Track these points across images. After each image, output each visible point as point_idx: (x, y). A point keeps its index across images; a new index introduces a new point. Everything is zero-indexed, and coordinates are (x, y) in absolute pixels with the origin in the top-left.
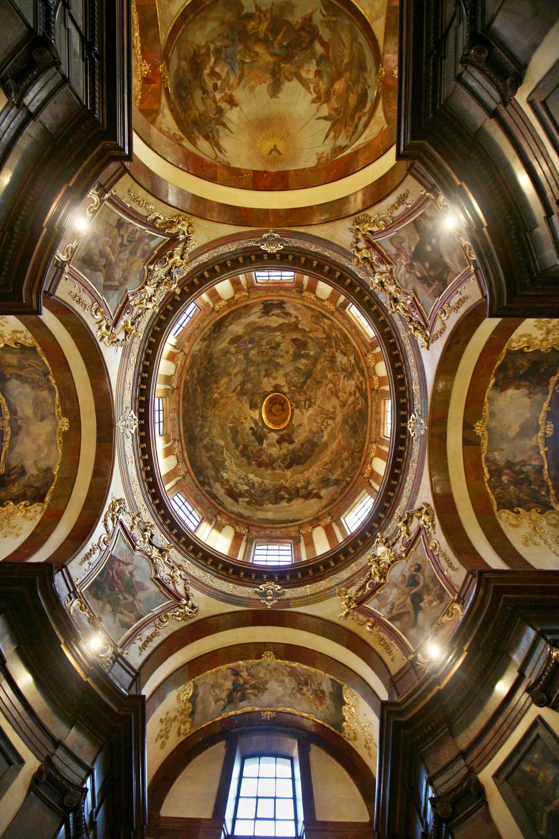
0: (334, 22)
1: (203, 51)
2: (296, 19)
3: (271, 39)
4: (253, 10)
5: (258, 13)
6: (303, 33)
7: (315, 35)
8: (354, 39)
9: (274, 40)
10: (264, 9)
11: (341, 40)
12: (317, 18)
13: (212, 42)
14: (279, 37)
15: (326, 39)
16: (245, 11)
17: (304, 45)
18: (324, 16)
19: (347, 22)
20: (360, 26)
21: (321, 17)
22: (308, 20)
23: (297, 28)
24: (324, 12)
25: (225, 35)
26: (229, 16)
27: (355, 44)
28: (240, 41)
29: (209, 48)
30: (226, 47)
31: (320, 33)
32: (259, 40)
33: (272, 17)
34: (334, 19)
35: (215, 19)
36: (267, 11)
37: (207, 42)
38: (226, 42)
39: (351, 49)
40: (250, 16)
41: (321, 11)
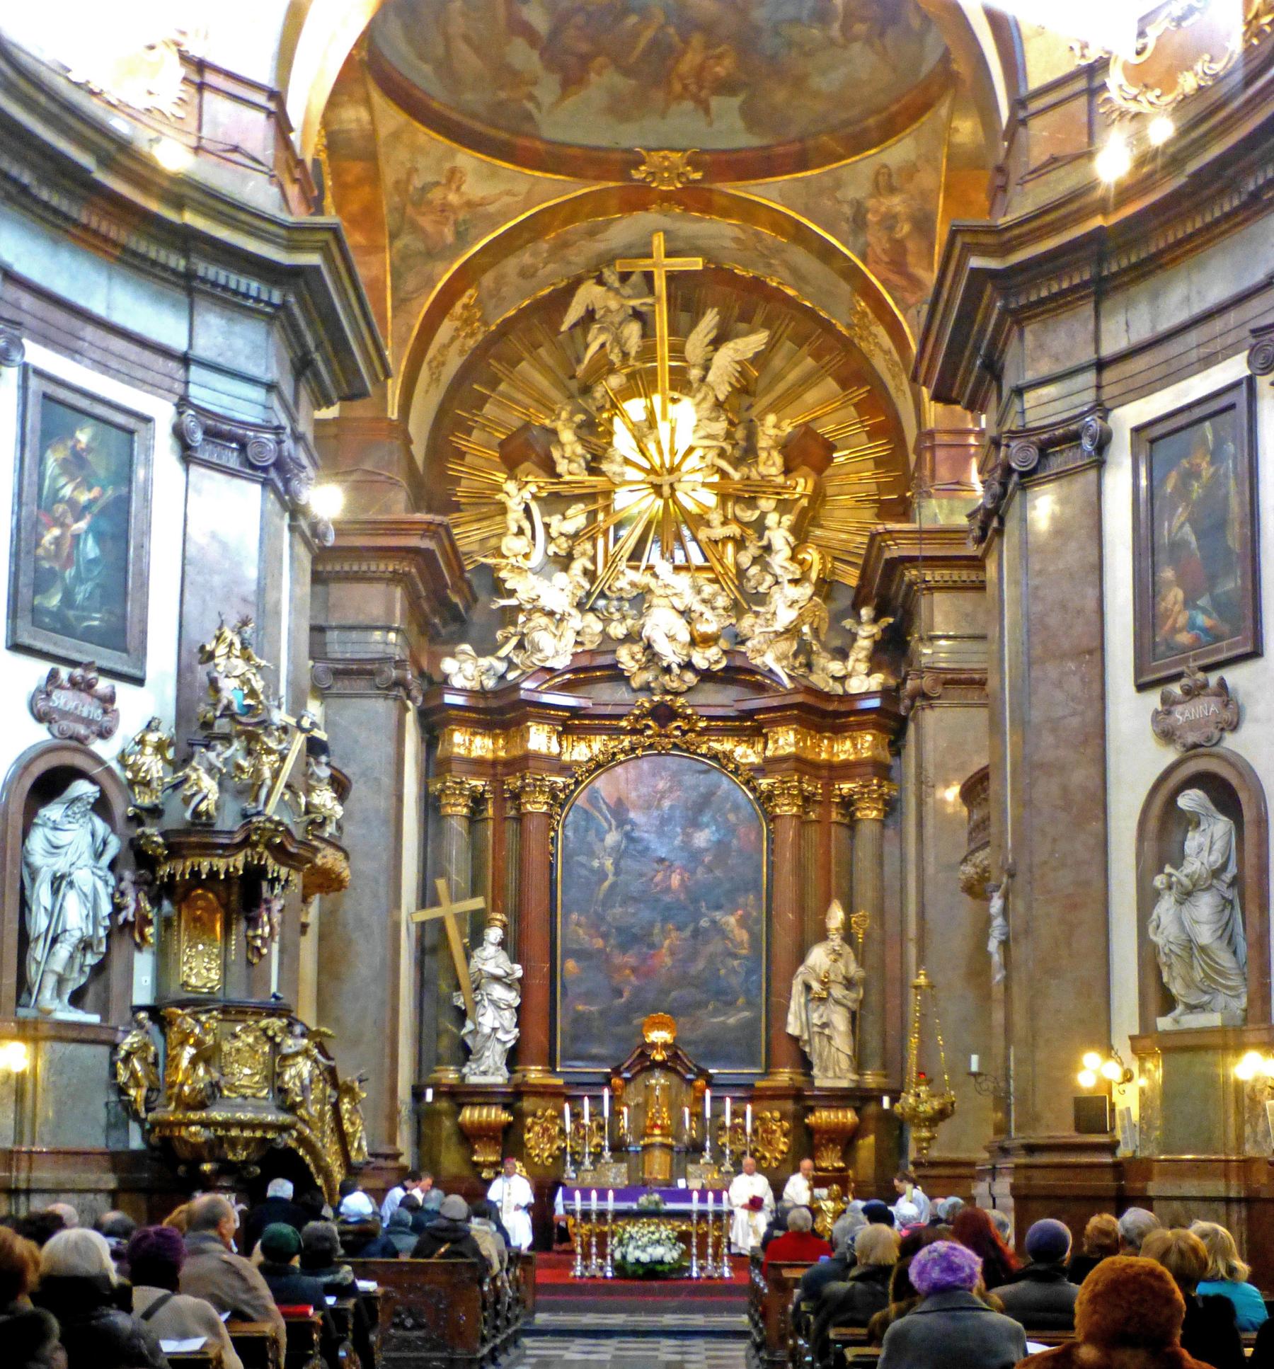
0: (502, 88)
1: (860, 28)
2: (605, 81)
3: (671, 30)
4: (715, 102)
5: (703, 94)
6: (584, 47)
7: (550, 49)
8: (445, 68)
9: (662, 27)
10: (688, 105)
11: (477, 50)
12: (548, 89)
13: (832, 42)
14: (648, 34)
15: (520, 43)
16: (736, 101)
17: (580, 19)
18: (531, 97)
19: (469, 96)
20: (435, 105)
21: (537, 92)
22: (572, 80)
23: (600, 60)
24: (530, 106)
25: (794, 53)
26: (781, 96)
27: (440, 51)
28: (758, 30)
29: (845, 28)
30: (796, 21)
31: (535, 55)
32: (708, 29)
33: (669, 83)
34: (503, 95)
35: (816, 95)
36: (680, 98)
37: (845, 47)
38: (796, 33)
39: (447, 40)
40: (726, 87)
41: (539, 106)
